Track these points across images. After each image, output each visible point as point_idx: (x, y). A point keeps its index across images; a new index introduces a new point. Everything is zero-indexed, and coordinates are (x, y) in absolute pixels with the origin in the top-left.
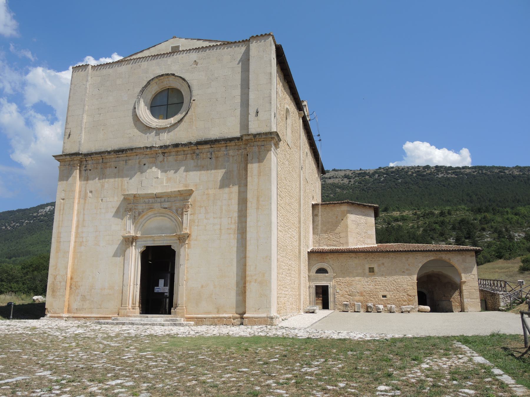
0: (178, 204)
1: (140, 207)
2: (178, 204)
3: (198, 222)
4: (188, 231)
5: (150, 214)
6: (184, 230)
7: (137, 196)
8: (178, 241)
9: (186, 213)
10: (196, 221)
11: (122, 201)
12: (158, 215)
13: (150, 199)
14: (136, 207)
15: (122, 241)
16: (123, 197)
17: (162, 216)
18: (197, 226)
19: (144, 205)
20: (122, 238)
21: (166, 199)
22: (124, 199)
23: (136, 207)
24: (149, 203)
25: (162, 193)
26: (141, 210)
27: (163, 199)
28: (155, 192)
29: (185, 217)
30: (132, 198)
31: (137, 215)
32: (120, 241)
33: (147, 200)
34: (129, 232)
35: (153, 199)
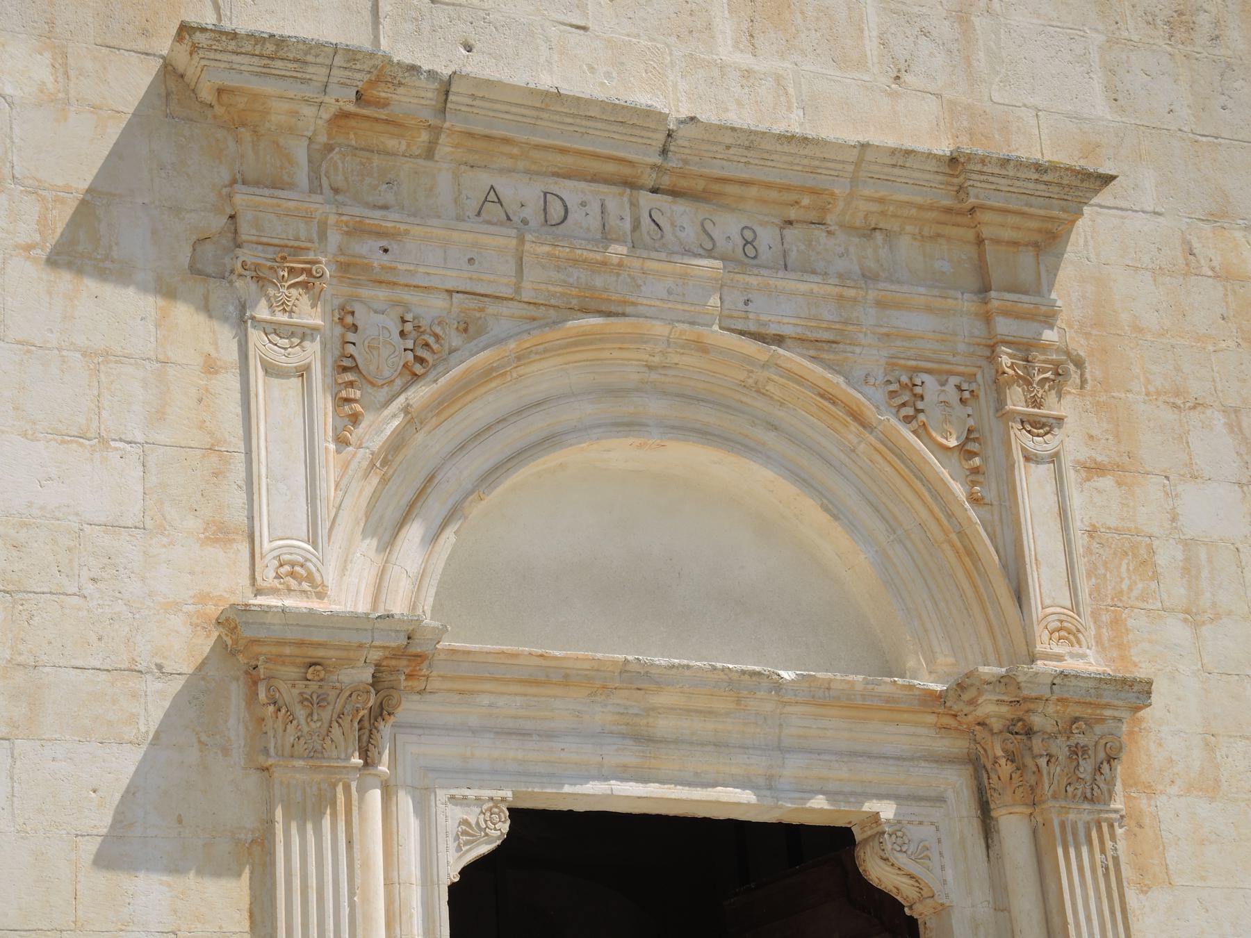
0: (918, 323)
1: (439, 260)
2: (918, 323)
3: (1189, 569)
4: (1088, 661)
5: (545, 376)
6: (1044, 644)
7: (411, 101)
8: (956, 785)
9: (1038, 445)
10: (1168, 555)
11: (140, 122)
12: (655, 407)
13: (572, 192)
14: (367, 249)
15: (199, 696)
16: (132, 82)
17: (704, 434)
18: (1192, 616)
19: (504, 240)
20: (184, 646)
21: (766, 237)
22: (172, 85)
23: (367, 249)
24: (555, 221)
25: (750, 140)
26: (432, 307)
27: (728, 227)
28: (674, 97)
29: (1034, 490)
30: (313, 119)
31: (383, 350)
32: (153, 704)
33: (522, 192)
34: (297, 573)
35: (616, 201)
